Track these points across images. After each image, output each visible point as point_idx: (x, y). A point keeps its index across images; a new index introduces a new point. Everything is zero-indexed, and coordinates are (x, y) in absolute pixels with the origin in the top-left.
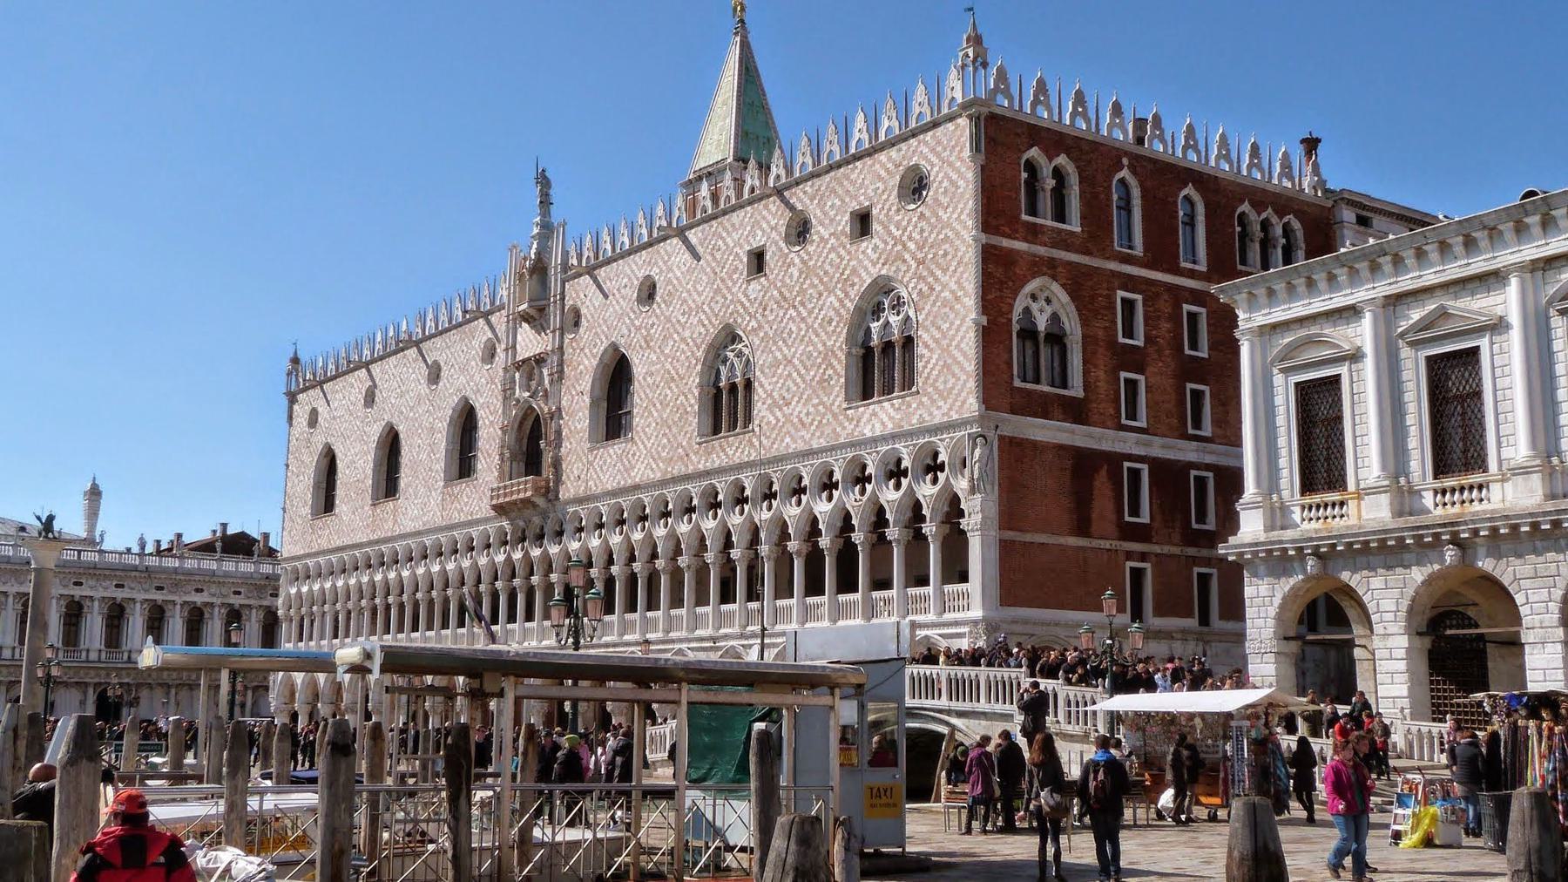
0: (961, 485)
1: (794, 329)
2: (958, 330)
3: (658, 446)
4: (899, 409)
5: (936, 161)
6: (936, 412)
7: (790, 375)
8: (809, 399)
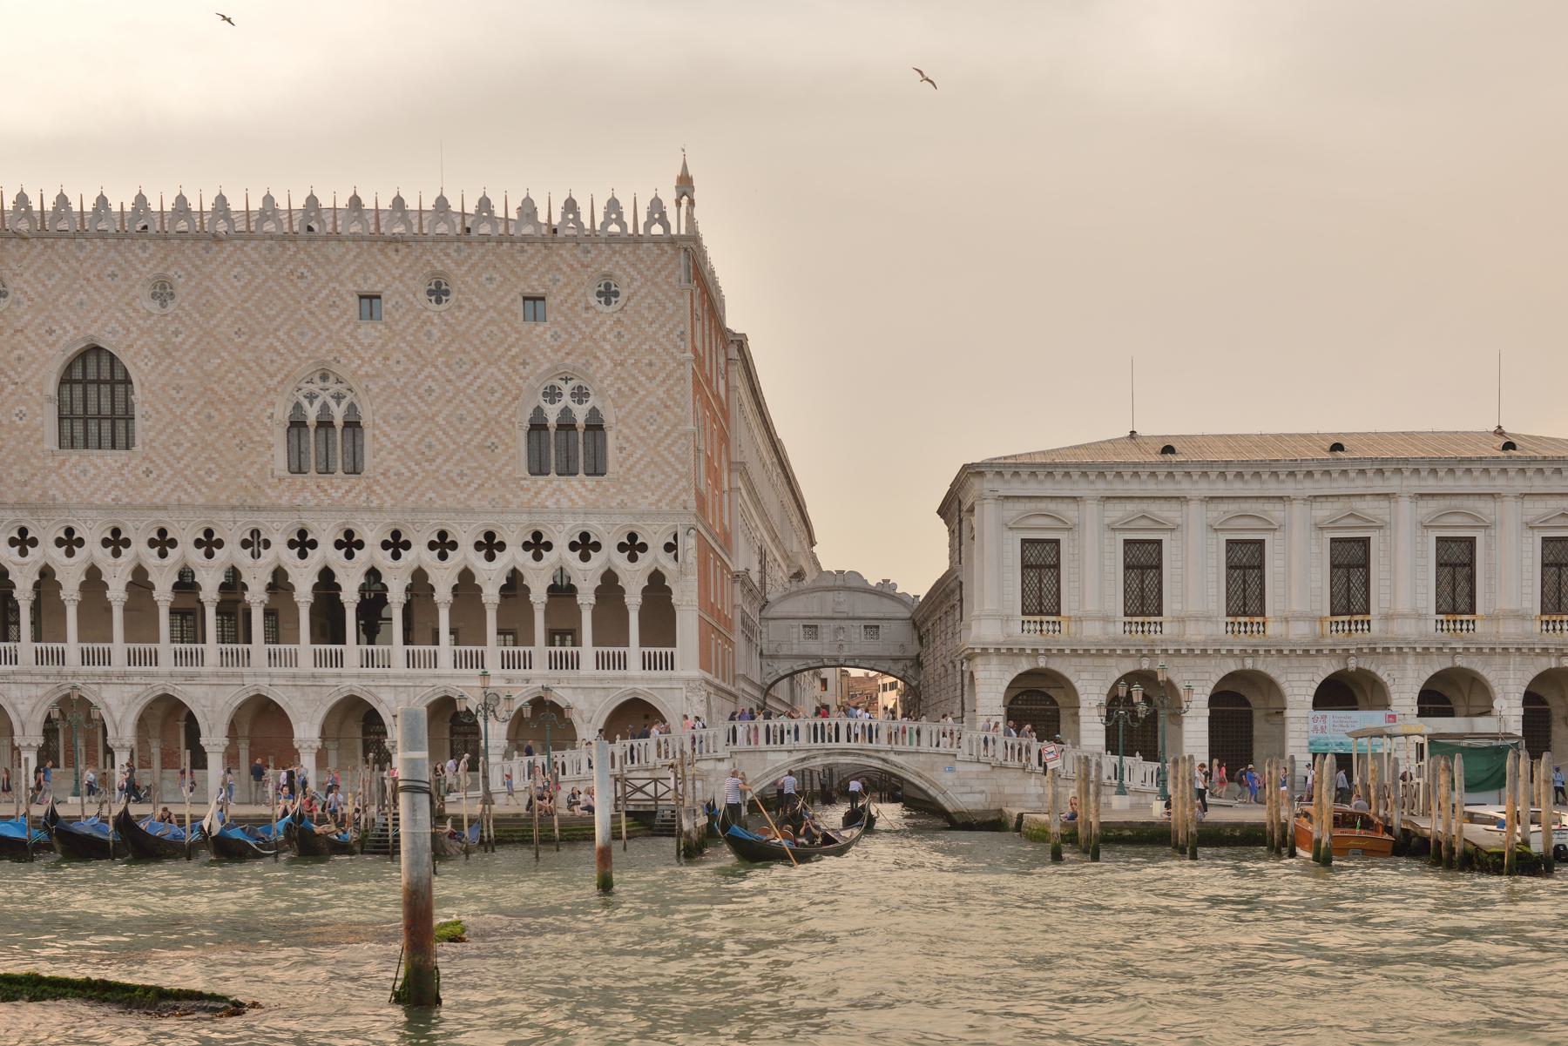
0: (666, 563)
1: (435, 387)
2: (667, 434)
3: (200, 469)
4: (593, 490)
5: (634, 273)
6: (640, 501)
7: (433, 434)
8: (462, 460)
